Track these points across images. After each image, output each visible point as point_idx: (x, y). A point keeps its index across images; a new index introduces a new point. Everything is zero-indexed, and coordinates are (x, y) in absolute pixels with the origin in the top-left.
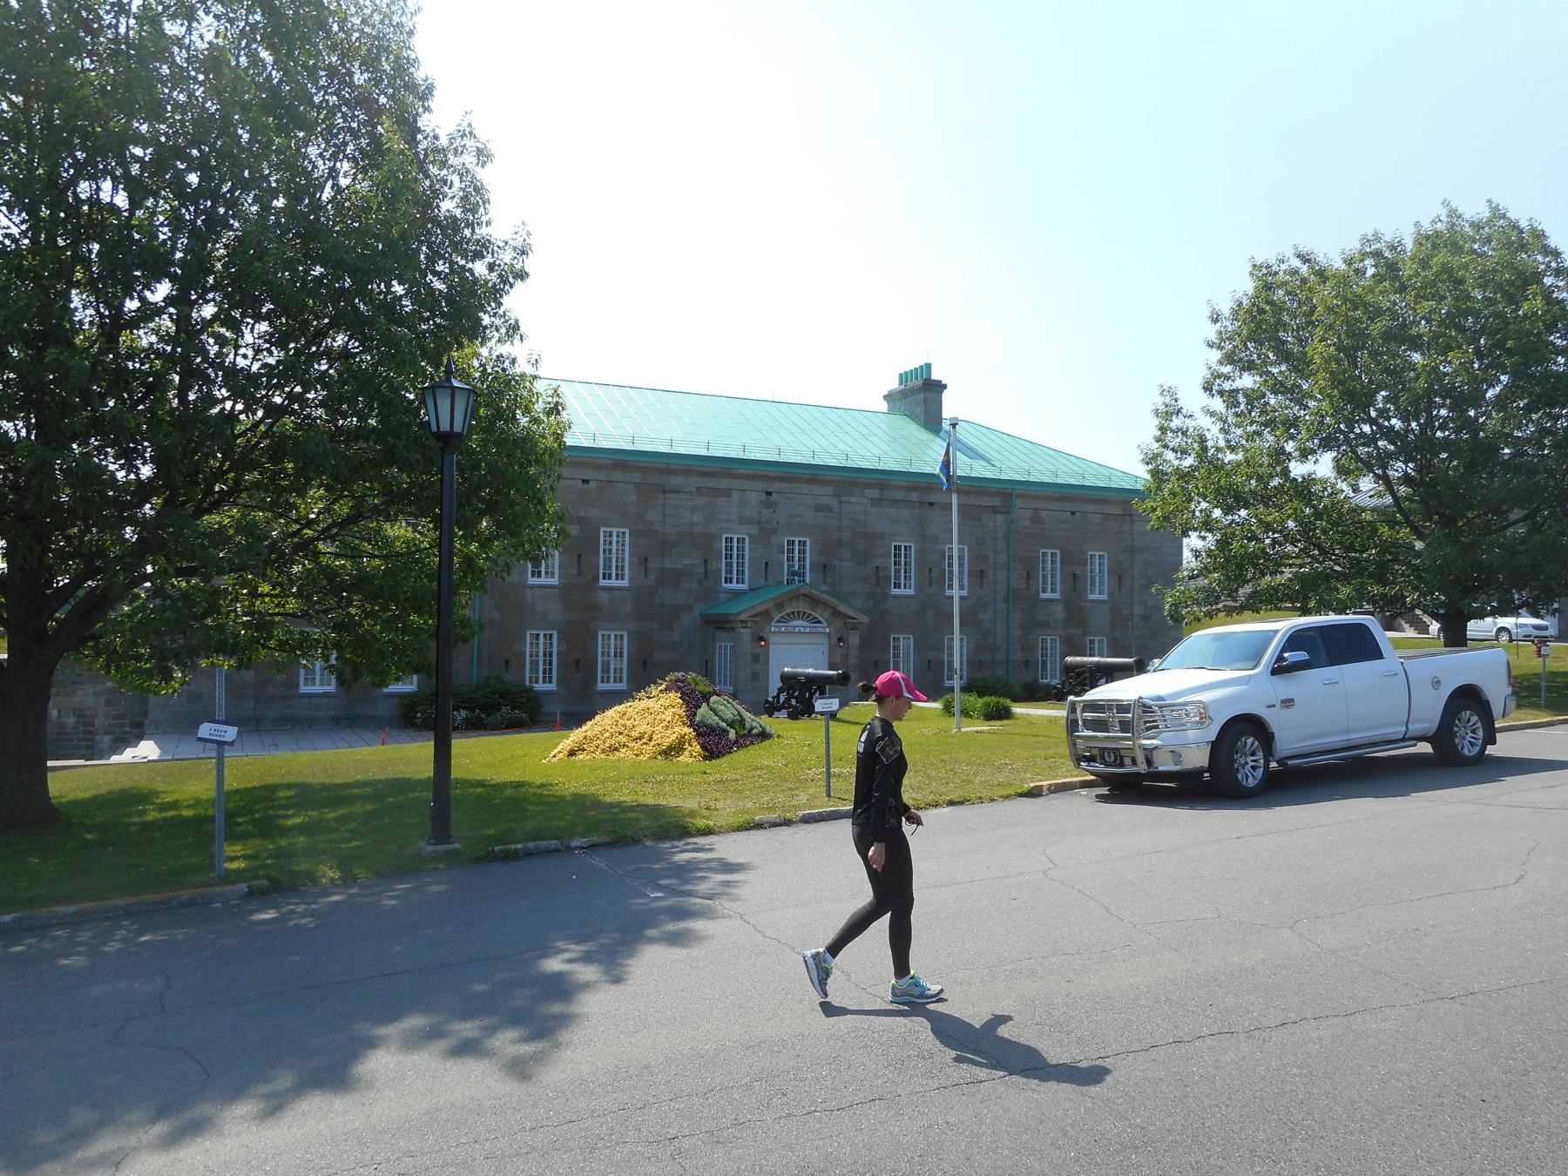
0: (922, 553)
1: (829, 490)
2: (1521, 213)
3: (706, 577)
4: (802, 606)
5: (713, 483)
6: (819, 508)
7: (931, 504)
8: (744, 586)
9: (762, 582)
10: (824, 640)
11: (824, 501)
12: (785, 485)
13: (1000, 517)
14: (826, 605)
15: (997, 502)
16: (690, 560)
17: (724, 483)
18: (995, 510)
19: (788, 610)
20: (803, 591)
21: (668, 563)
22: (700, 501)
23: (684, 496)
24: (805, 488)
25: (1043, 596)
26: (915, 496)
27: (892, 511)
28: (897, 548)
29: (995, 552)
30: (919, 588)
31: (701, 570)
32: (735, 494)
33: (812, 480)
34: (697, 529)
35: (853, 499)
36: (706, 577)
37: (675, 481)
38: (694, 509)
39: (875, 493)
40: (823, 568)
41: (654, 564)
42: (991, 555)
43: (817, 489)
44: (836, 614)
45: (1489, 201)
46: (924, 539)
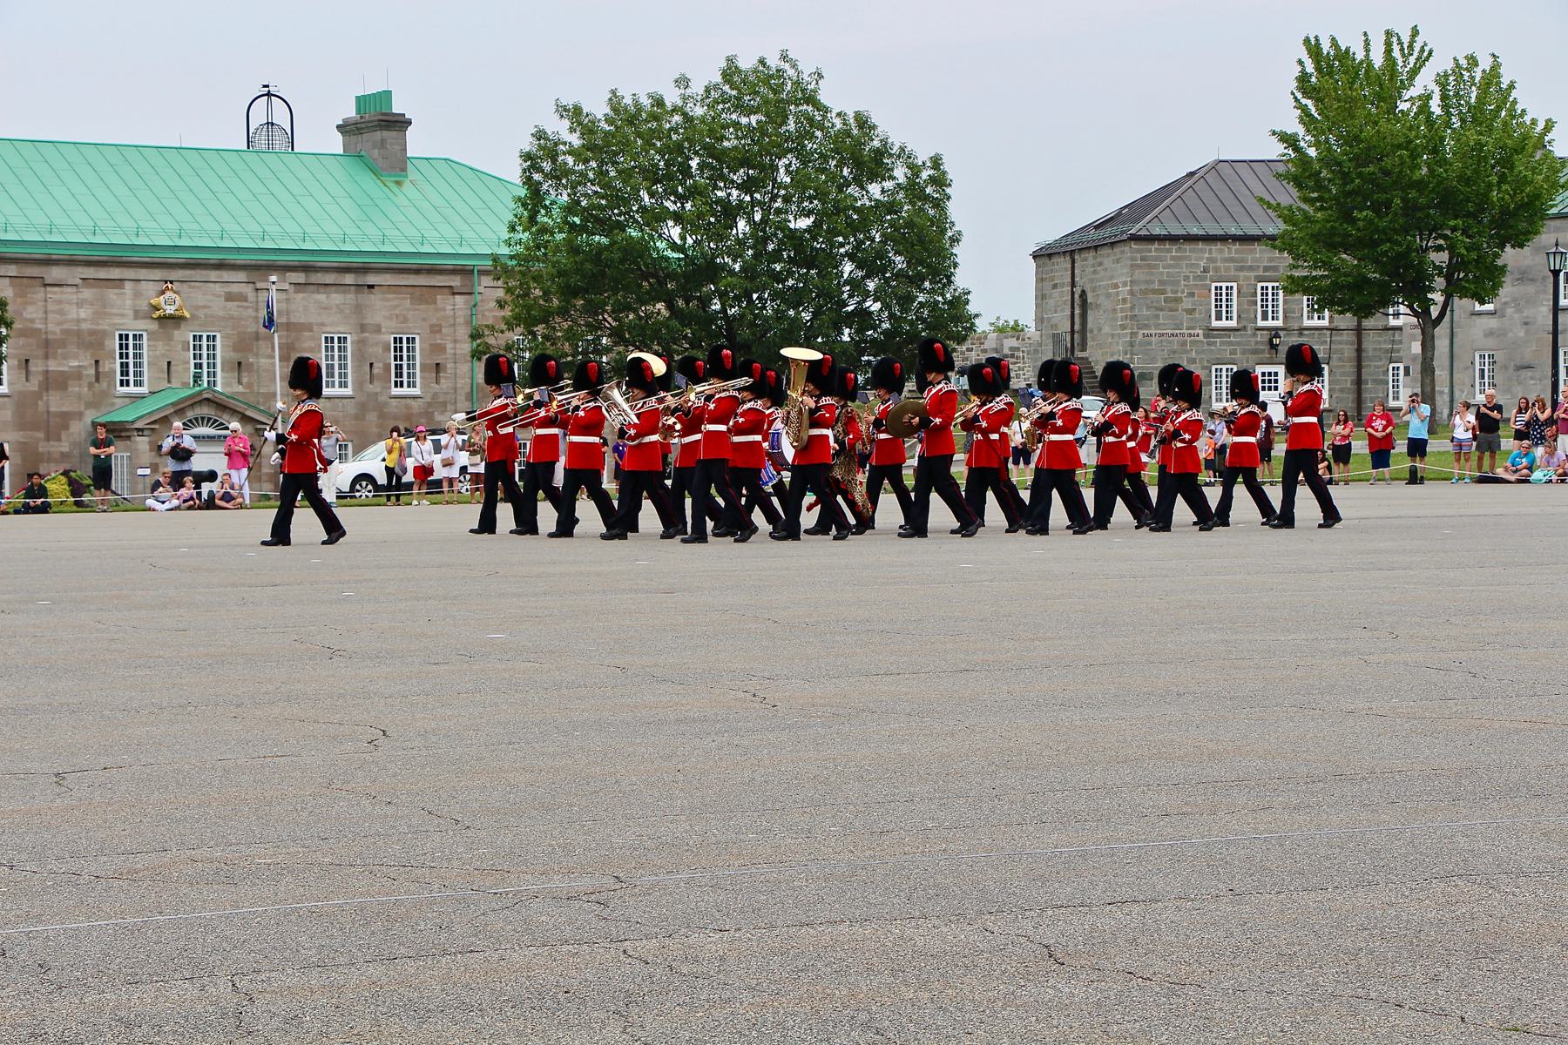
0: (360, 344)
1: (241, 276)
2: (752, 51)
3: (97, 380)
5: (102, 273)
7: (371, 287)
8: (144, 390)
9: (165, 385)
11: (235, 288)
12: (188, 272)
16: (79, 361)
17: (115, 273)
21: (53, 366)
22: (87, 293)
23: (69, 289)
24: (213, 275)
26: (349, 279)
27: (322, 297)
29: (455, 341)
30: (359, 385)
31: (92, 372)
32: (128, 285)
33: (221, 266)
34: (85, 326)
36: (97, 380)
37: (56, 273)
38: (79, 305)
39: (299, 277)
41: (37, 367)
42: (449, 346)
43: (226, 275)
45: (614, 92)
46: (363, 328)
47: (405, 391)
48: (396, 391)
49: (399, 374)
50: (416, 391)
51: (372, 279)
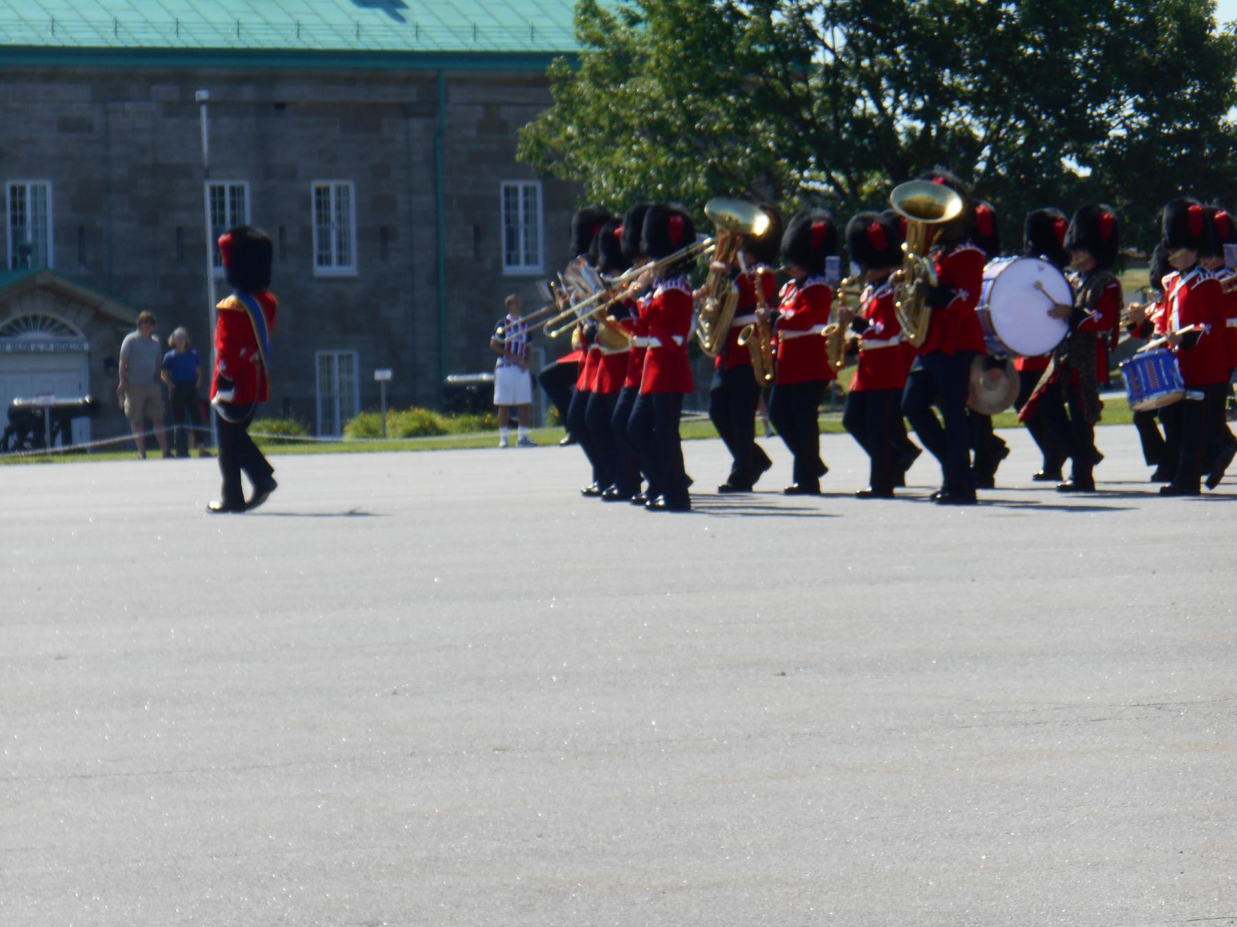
4: (39, 307)
6: (66, 125)
7: (280, 106)
10: (80, 363)
13: (417, 124)
14: (82, 304)
15: (411, 95)
18: (406, 111)
19: (17, 314)
20: (41, 280)
25: (509, 270)
26: (248, 93)
28: (218, 192)
33: (51, 77)
35: (129, 106)
40: (76, 235)
44: (101, 318)
47: (334, 270)
48: (320, 271)
49: (324, 244)
50: (350, 270)
51: (283, 93)
